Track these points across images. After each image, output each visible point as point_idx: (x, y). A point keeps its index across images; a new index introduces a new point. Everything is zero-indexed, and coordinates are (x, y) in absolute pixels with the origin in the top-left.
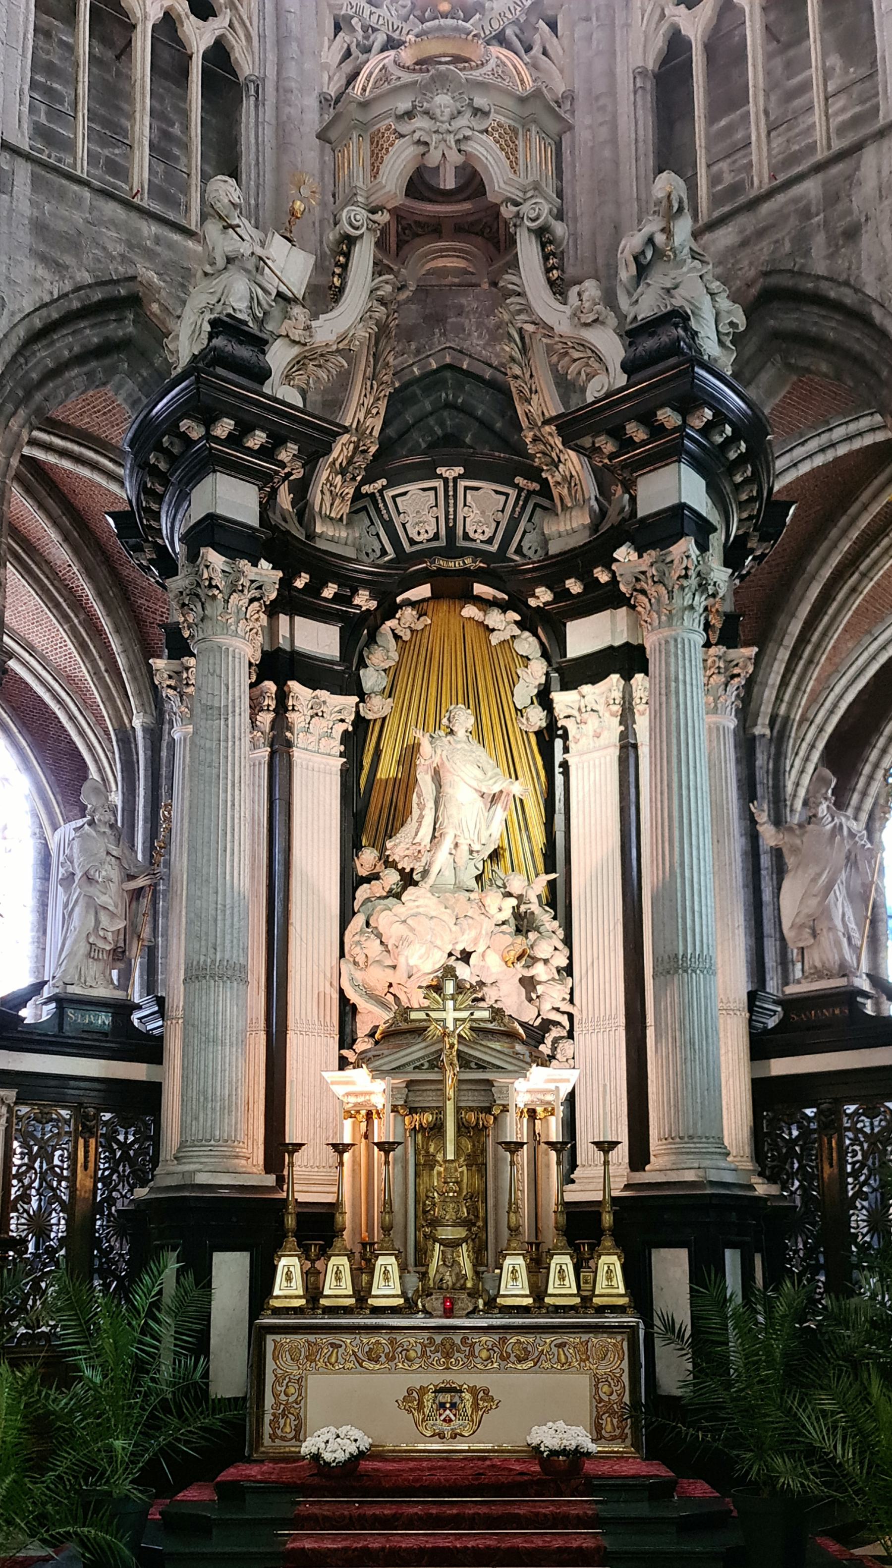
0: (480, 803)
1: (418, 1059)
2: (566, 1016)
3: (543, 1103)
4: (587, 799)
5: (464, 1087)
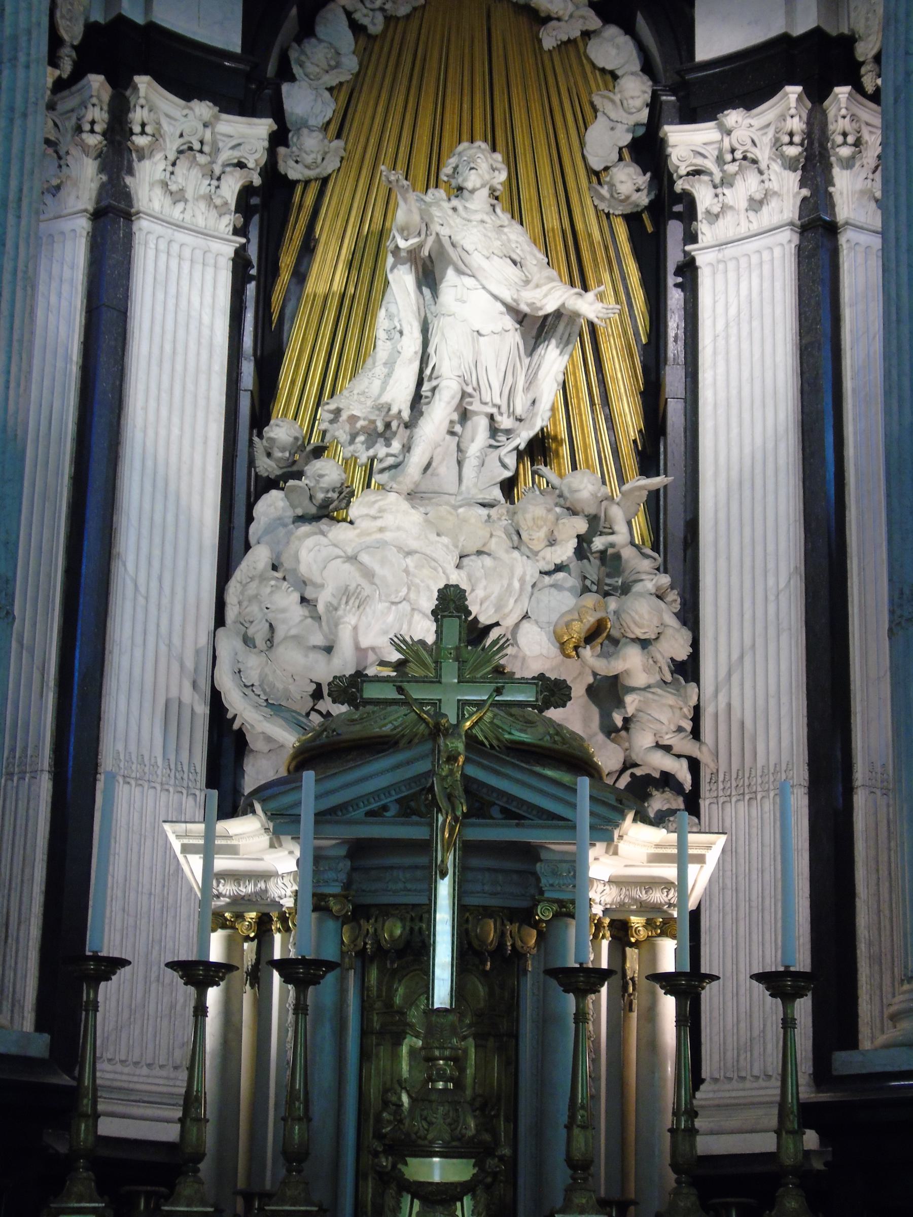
0: (514, 338)
1: (376, 794)
2: (684, 763)
3: (645, 908)
4: (733, 331)
5: (475, 862)
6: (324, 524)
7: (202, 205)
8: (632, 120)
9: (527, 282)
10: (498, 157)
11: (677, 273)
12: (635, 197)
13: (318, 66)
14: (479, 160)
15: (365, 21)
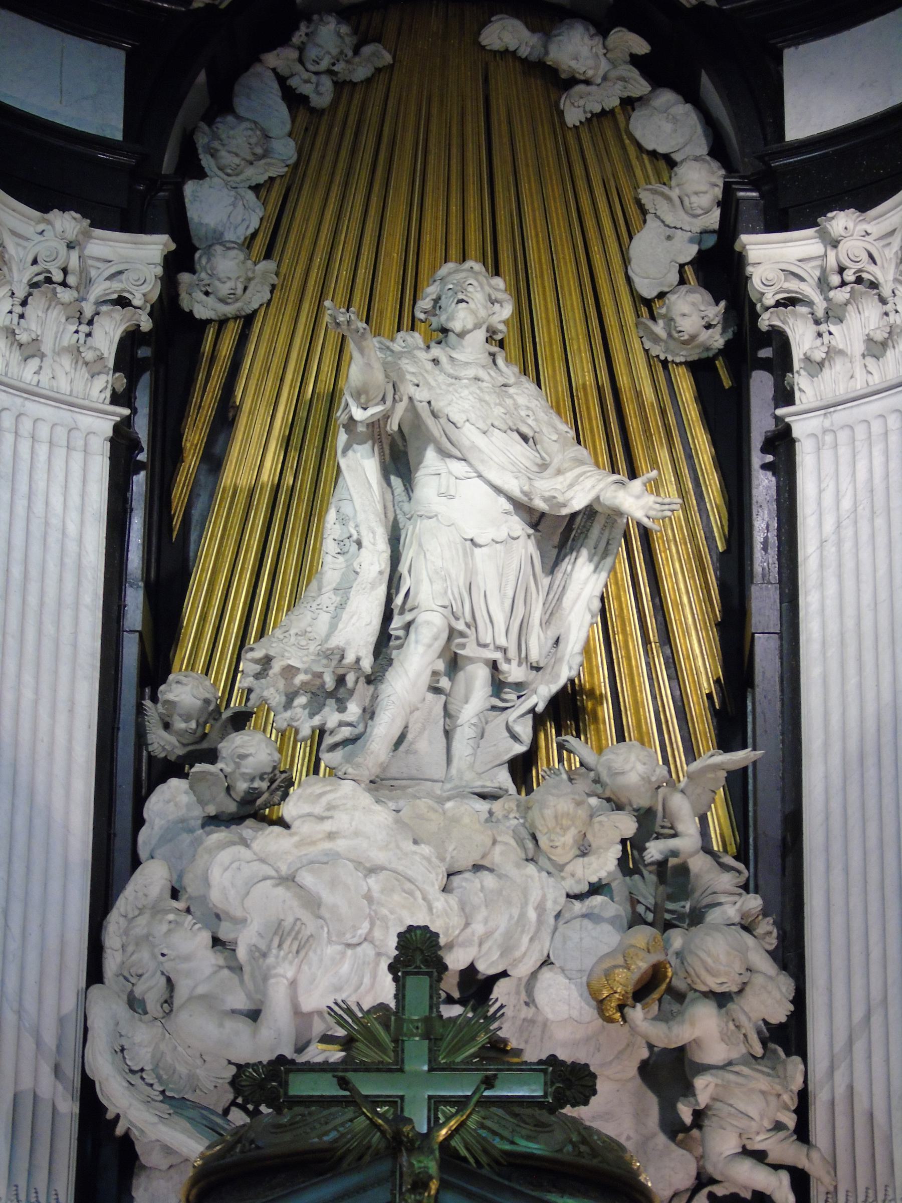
2: (784, 1178)
4: (848, 533)
6: (247, 829)
7: (66, 362)
8: (698, 225)
9: (543, 466)
11: (765, 450)
12: (704, 335)
13: (237, 155)
14: (470, 289)
15: (306, 89)
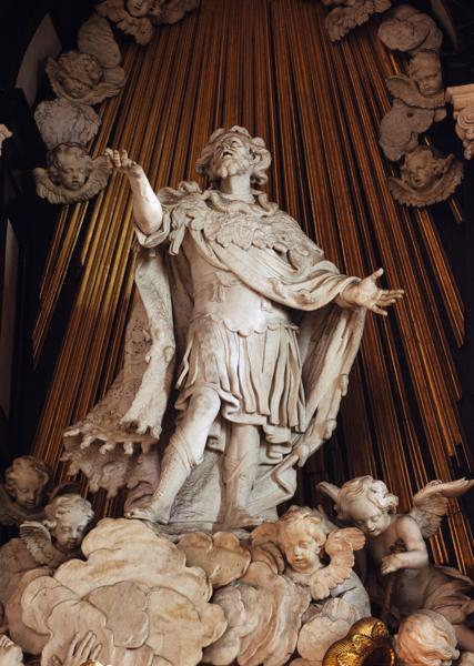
10: (259, 141)
13: (79, 81)
14: (235, 145)
15: (132, 31)
